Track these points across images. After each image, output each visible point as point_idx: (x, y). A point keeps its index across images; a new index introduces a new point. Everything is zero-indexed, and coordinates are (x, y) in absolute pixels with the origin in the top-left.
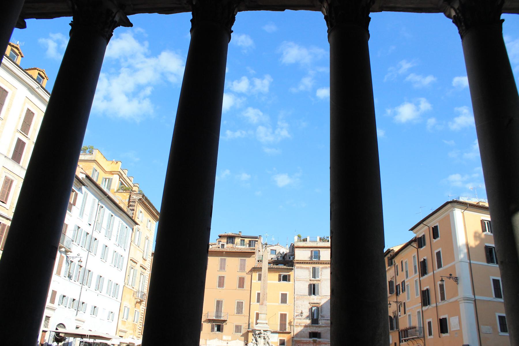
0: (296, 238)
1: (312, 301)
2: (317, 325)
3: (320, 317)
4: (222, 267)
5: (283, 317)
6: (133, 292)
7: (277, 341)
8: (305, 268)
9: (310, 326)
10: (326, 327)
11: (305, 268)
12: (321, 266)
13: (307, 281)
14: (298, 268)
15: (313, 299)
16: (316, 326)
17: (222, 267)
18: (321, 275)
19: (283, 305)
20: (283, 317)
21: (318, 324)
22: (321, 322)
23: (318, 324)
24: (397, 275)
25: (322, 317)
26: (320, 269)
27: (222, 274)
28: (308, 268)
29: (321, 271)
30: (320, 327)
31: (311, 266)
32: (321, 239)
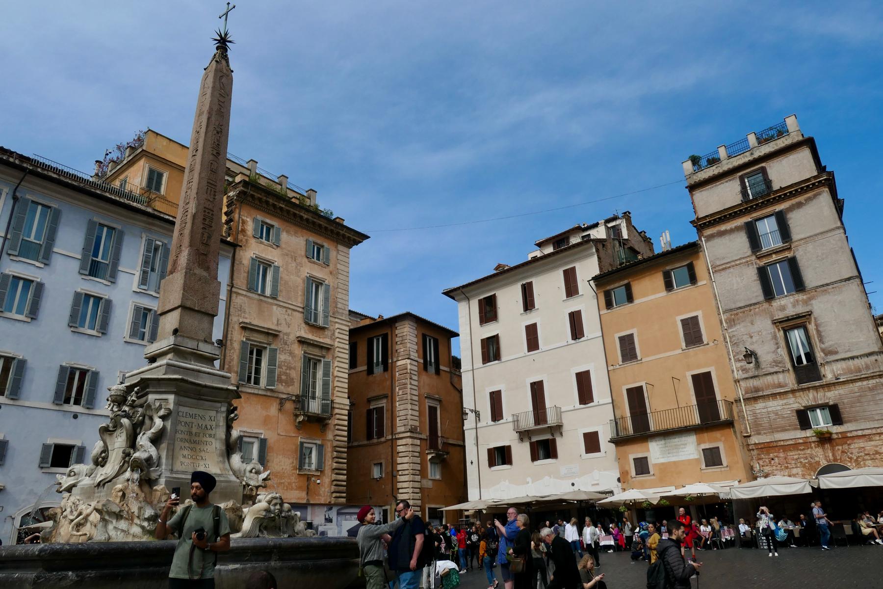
0: (688, 166)
1: (780, 315)
2: (817, 383)
4: (528, 304)
5: (703, 383)
6: (278, 401)
7: (696, 457)
8: (731, 231)
9: (793, 391)
11: (731, 231)
14: (710, 238)
15: (783, 308)
16: (815, 388)
17: (528, 304)
19: (694, 351)
20: (703, 383)
21: (819, 378)
22: (828, 373)
23: (819, 378)
25: (827, 352)
27: (531, 318)
30: (829, 386)
32: (761, 141)
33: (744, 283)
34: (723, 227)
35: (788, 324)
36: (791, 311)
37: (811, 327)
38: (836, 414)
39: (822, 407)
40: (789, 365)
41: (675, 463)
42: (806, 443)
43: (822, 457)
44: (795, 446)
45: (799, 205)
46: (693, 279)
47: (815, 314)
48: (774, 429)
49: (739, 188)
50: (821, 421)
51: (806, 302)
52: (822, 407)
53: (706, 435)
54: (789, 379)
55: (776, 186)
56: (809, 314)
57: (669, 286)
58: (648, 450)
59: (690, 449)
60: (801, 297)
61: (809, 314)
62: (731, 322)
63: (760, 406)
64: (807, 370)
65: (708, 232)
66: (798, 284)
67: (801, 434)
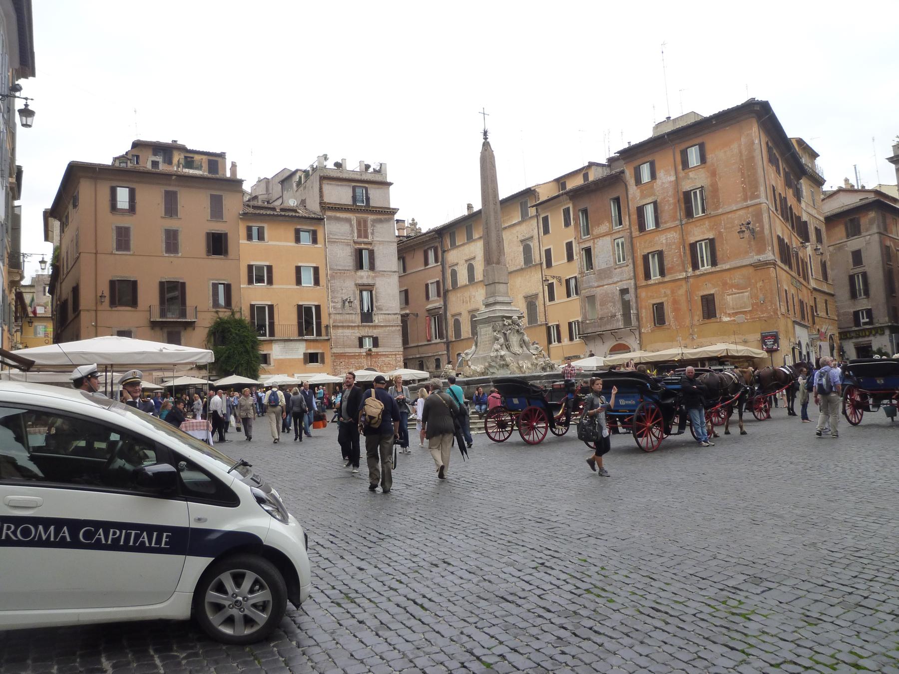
1: (360, 282)
2: (371, 324)
3: (375, 309)
4: (171, 209)
9: (358, 326)
10: (386, 326)
12: (371, 217)
13: (348, 245)
14: (329, 218)
15: (362, 277)
16: (369, 326)
18: (372, 234)
22: (377, 319)
24: (546, 231)
25: (379, 309)
26: (369, 224)
27: (172, 224)
28: (349, 221)
29: (373, 226)
30: (375, 327)
31: (353, 217)
33: (343, 256)
34: (339, 215)
35: (362, 288)
36: (365, 281)
37: (374, 292)
38: (376, 342)
39: (369, 337)
40: (359, 311)
41: (290, 360)
42: (360, 355)
43: (365, 362)
44: (353, 356)
45: (381, 221)
46: (315, 241)
47: (377, 285)
48: (344, 346)
49: (351, 194)
50: (368, 343)
51: (373, 278)
52: (369, 337)
53: (312, 344)
54: (358, 319)
55: (372, 204)
56: (373, 285)
57: (298, 240)
58: (271, 349)
59: (300, 350)
60: (371, 273)
61: (373, 285)
62: (333, 277)
63: (340, 331)
64: (367, 317)
65: (329, 213)
66: (372, 267)
67: (358, 350)
